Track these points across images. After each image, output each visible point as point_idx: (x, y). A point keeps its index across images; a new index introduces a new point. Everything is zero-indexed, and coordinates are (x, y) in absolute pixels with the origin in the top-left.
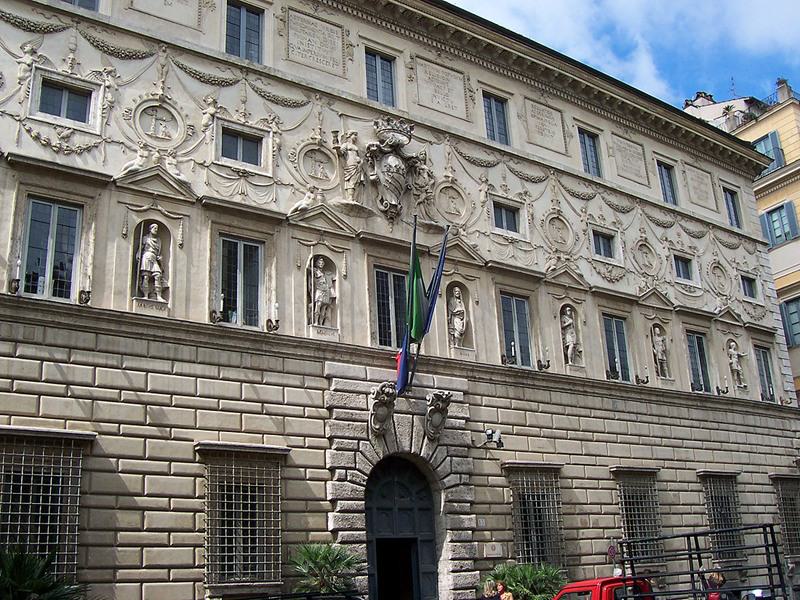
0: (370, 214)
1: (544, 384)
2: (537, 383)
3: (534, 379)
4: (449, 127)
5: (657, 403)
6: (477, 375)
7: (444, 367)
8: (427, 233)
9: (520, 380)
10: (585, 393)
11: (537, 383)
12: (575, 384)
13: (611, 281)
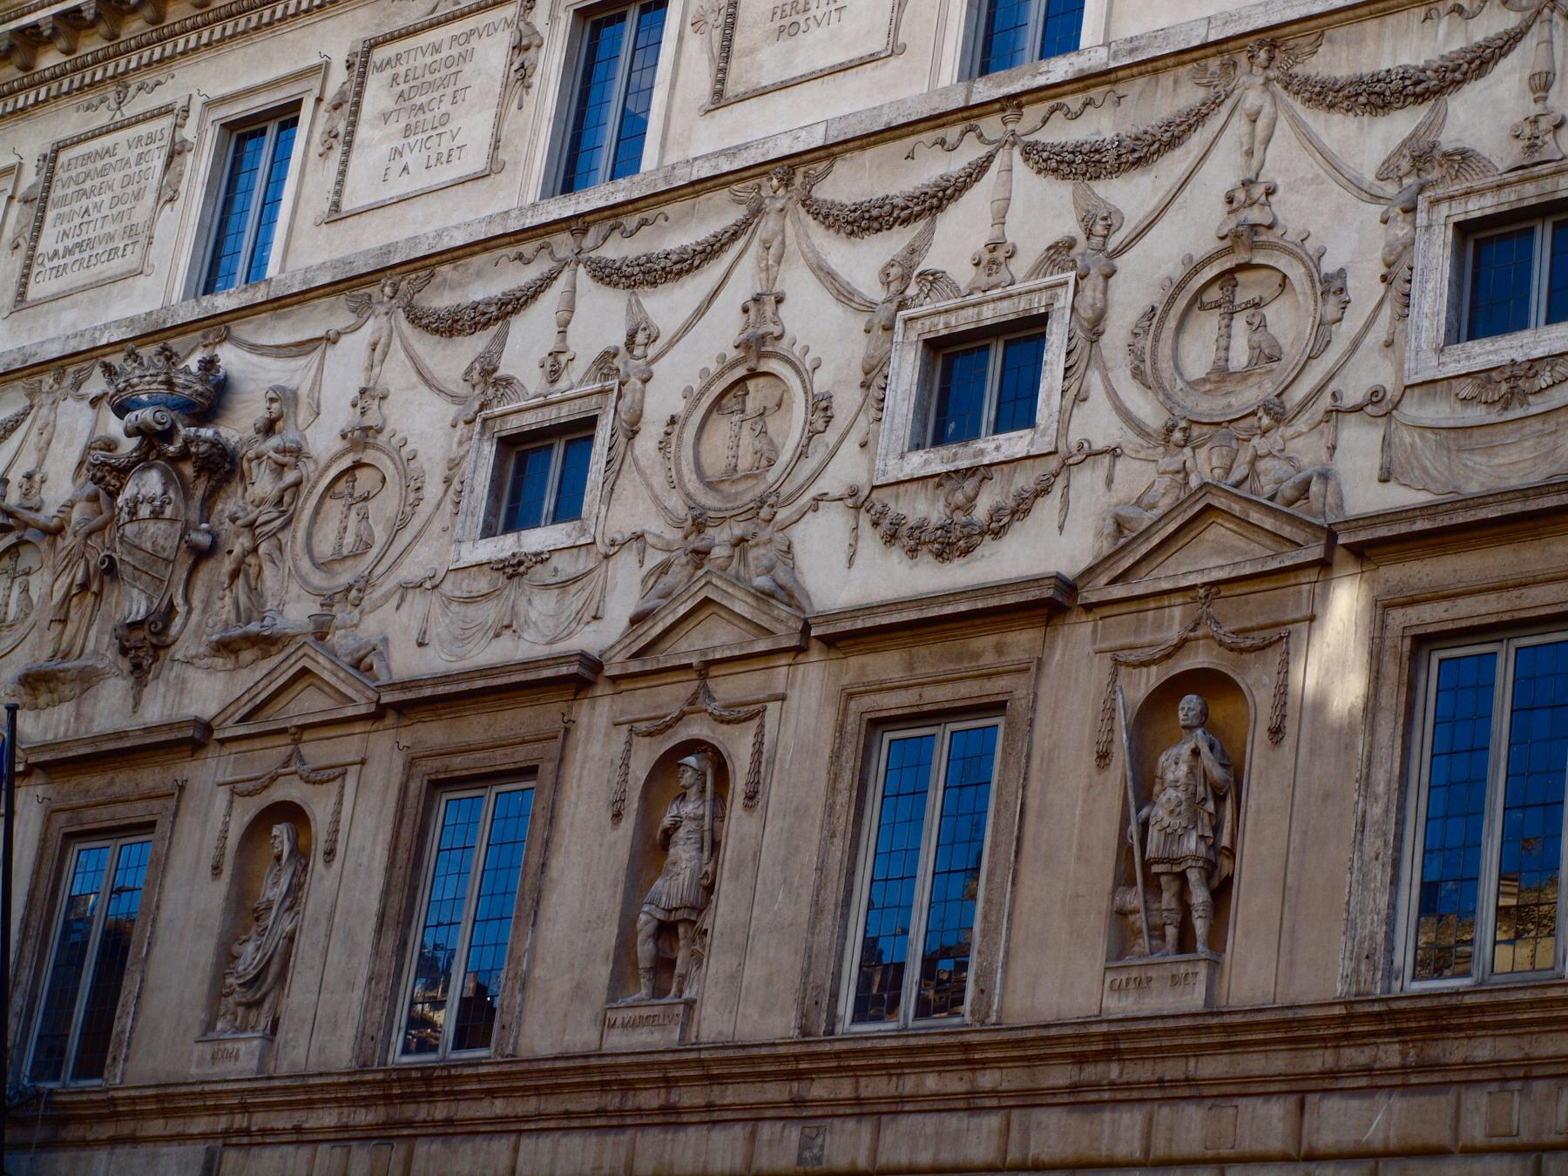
0: (88, 679)
1: (499, 1107)
2: (466, 1110)
3: (455, 1096)
4: (388, 250)
5: (1078, 1099)
6: (259, 1120)
7: (164, 1113)
8: (238, 667)
9: (408, 1111)
10: (670, 1118)
11: (466, 1110)
12: (627, 1086)
13: (950, 543)
